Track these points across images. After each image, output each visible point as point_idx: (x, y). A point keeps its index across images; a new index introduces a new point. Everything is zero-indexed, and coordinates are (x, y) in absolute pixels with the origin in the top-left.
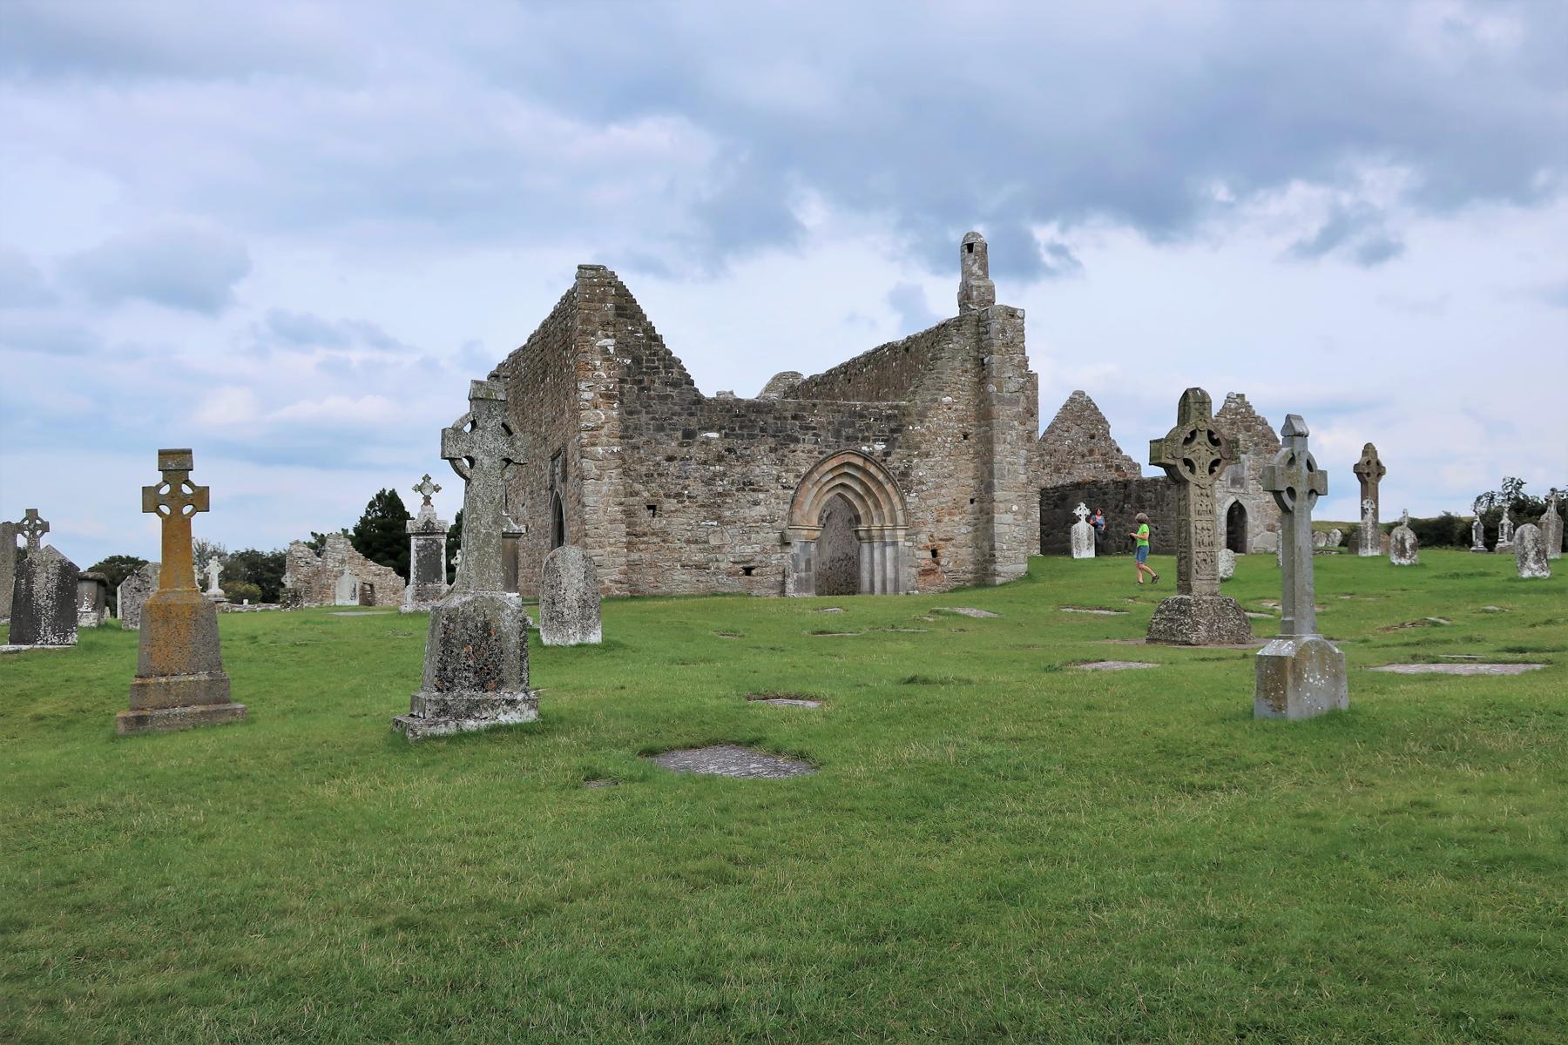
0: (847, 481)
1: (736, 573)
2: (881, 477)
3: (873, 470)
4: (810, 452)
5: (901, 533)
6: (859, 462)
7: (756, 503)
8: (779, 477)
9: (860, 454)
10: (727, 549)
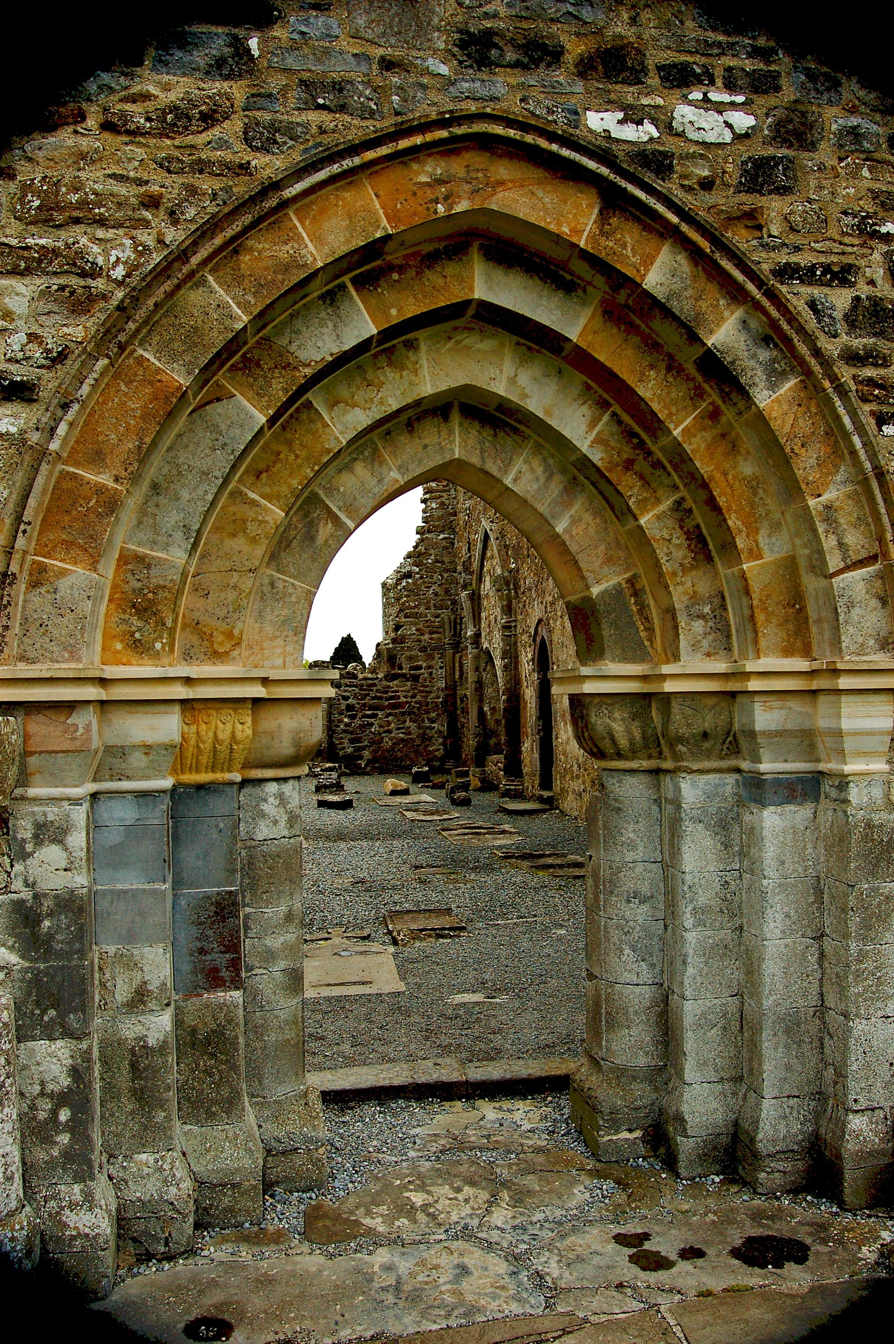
0: (503, 375)
2: (726, 333)
3: (661, 273)
6: (572, 218)
9: (556, 159)
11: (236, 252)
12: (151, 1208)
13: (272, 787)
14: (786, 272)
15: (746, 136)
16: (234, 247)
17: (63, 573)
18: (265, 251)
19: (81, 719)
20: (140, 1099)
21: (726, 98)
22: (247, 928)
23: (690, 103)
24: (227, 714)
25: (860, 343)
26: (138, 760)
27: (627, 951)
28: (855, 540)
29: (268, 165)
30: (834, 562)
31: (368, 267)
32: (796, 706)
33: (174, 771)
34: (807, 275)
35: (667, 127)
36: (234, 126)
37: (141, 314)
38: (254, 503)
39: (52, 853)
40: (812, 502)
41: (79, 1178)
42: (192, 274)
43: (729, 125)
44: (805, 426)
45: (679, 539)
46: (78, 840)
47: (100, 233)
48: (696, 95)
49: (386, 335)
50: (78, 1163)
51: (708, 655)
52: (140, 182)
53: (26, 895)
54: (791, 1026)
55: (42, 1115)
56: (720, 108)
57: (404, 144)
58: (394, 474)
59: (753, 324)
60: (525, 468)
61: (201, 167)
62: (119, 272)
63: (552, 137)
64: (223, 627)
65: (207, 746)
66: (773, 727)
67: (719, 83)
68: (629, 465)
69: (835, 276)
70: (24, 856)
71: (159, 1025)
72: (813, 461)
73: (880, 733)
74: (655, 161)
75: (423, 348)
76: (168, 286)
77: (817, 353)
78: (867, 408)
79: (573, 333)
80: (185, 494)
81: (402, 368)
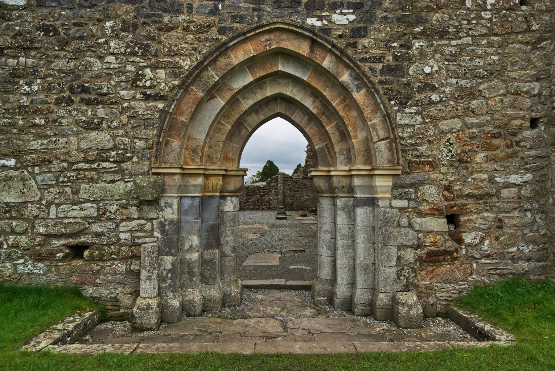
0: (289, 91)
1: (50, 256)
2: (345, 77)
3: (327, 63)
4: (203, 29)
5: (383, 184)
7: (92, 126)
8: (138, 77)
10: (31, 211)
11: (216, 61)
12: (191, 302)
13: (229, 198)
14: (363, 60)
15: (353, 21)
16: (215, 60)
17: (173, 142)
18: (222, 62)
19: (177, 177)
20: (189, 274)
21: (347, 11)
22: (221, 234)
23: (337, 14)
24: (215, 178)
25: (383, 78)
26: (192, 188)
27: (325, 247)
28: (382, 134)
29: (223, 38)
30: (375, 139)
31: (250, 64)
32: (367, 179)
33: (202, 192)
34: (369, 60)
35: (330, 22)
36: (214, 30)
37: (192, 78)
38: (224, 125)
39: (169, 210)
40: (369, 123)
41: (172, 292)
42: (204, 68)
43: (347, 19)
44: (367, 102)
45: (337, 133)
46: (175, 207)
47: (182, 58)
48: (338, 11)
49: (256, 81)
50: (173, 288)
51: (345, 165)
52: (192, 44)
53: (163, 220)
54: (366, 268)
55: (164, 275)
56: (345, 14)
57: (257, 31)
58: (262, 116)
59: (353, 74)
60: (297, 114)
61: (207, 40)
62: (187, 67)
63: (297, 27)
64: (215, 156)
65: (210, 186)
66: (360, 184)
67: (345, 7)
68: (323, 113)
69: (377, 60)
70: (162, 210)
71: (195, 256)
72: (369, 111)
73: (388, 186)
74: (326, 31)
75: (268, 83)
76: (198, 71)
77: (370, 82)
78: (386, 96)
79: (305, 79)
80: (205, 122)
81: (262, 89)
